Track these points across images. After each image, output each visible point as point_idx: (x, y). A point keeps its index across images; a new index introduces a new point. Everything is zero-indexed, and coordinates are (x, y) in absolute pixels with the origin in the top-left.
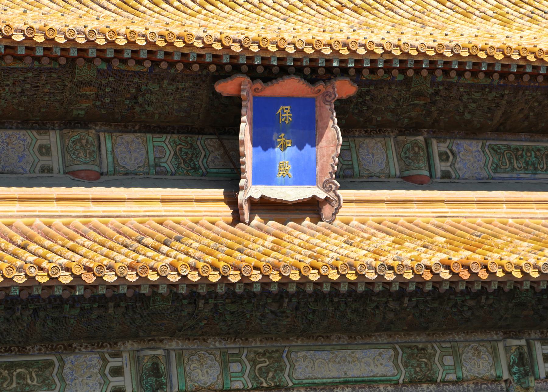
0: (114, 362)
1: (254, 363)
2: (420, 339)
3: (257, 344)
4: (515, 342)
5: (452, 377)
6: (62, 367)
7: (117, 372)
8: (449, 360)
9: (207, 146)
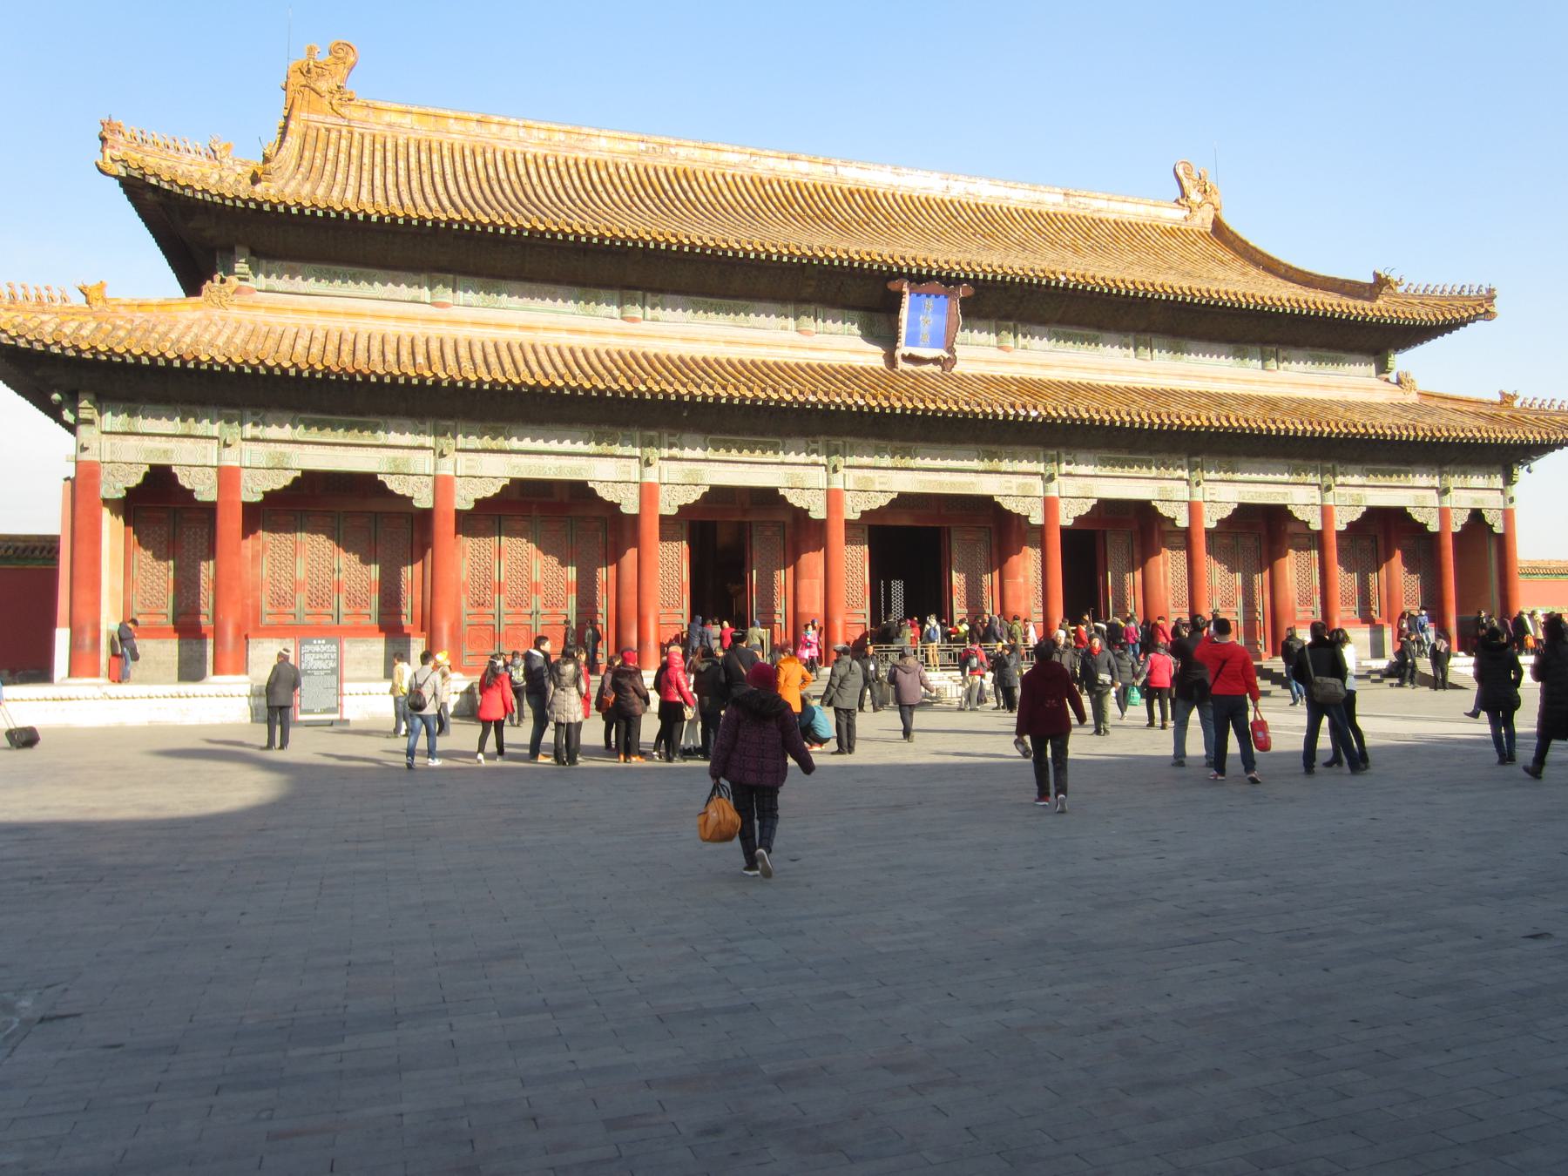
0: (814, 446)
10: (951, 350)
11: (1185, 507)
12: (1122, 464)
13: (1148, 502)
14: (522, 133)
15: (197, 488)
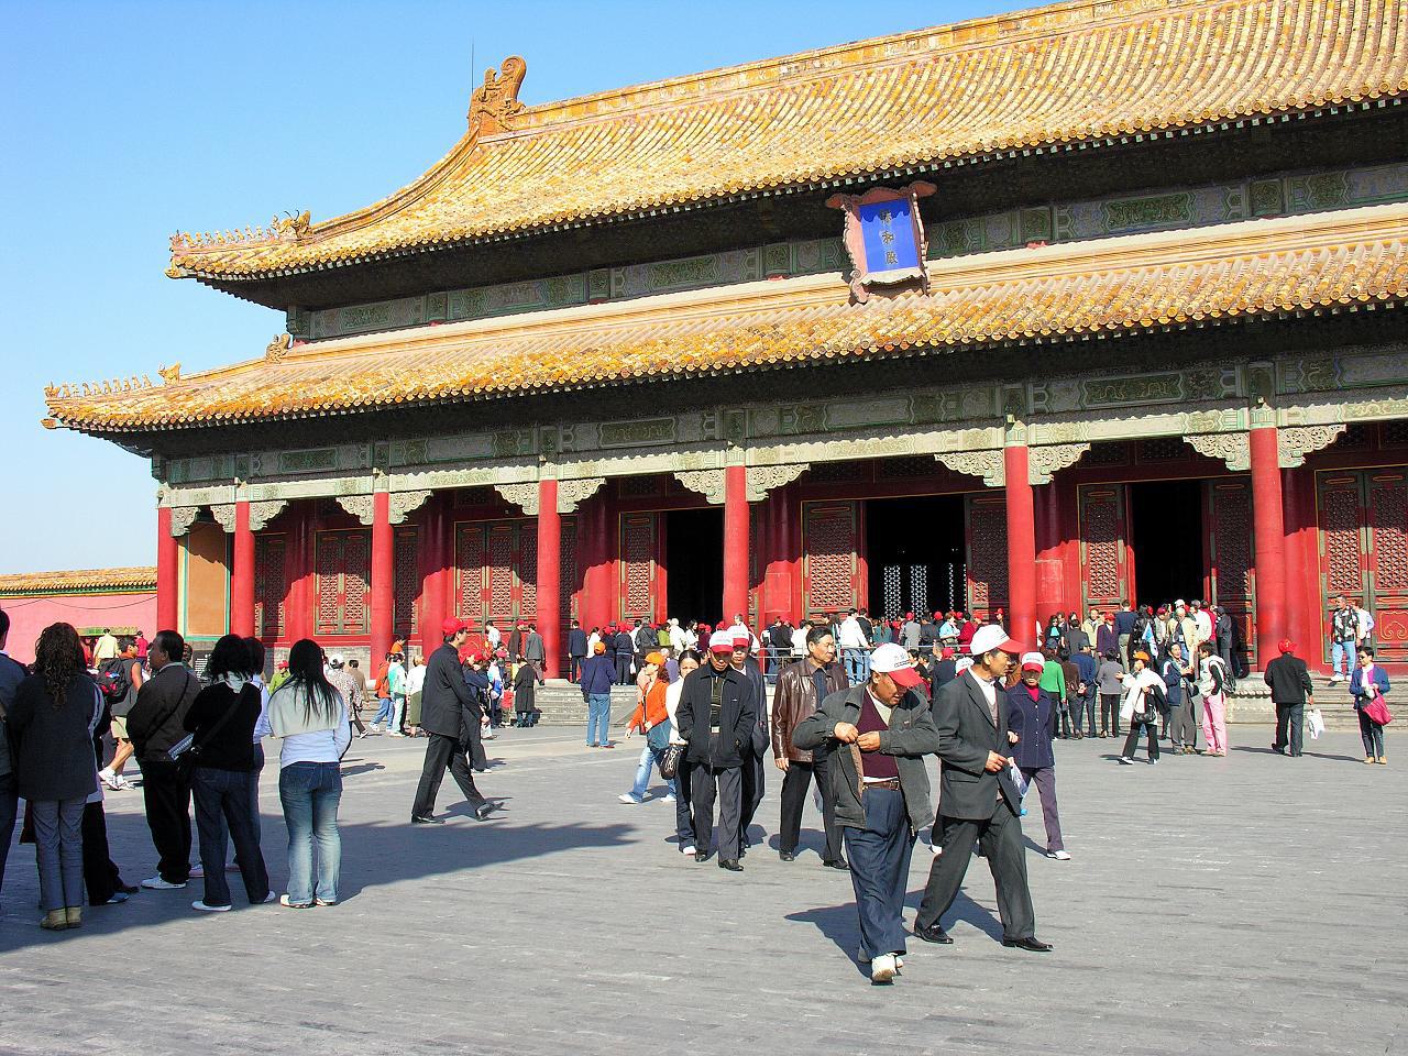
0: (709, 419)
1: (801, 415)
2: (932, 391)
3: (807, 402)
4: (1008, 387)
5: (954, 417)
6: (677, 425)
7: (711, 425)
8: (952, 405)
9: (817, 248)
10: (923, 269)
11: (1244, 439)
12: (1133, 389)
13: (1178, 439)
14: (663, 94)
15: (225, 522)
